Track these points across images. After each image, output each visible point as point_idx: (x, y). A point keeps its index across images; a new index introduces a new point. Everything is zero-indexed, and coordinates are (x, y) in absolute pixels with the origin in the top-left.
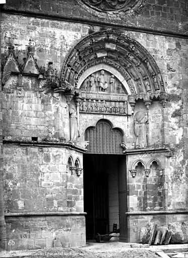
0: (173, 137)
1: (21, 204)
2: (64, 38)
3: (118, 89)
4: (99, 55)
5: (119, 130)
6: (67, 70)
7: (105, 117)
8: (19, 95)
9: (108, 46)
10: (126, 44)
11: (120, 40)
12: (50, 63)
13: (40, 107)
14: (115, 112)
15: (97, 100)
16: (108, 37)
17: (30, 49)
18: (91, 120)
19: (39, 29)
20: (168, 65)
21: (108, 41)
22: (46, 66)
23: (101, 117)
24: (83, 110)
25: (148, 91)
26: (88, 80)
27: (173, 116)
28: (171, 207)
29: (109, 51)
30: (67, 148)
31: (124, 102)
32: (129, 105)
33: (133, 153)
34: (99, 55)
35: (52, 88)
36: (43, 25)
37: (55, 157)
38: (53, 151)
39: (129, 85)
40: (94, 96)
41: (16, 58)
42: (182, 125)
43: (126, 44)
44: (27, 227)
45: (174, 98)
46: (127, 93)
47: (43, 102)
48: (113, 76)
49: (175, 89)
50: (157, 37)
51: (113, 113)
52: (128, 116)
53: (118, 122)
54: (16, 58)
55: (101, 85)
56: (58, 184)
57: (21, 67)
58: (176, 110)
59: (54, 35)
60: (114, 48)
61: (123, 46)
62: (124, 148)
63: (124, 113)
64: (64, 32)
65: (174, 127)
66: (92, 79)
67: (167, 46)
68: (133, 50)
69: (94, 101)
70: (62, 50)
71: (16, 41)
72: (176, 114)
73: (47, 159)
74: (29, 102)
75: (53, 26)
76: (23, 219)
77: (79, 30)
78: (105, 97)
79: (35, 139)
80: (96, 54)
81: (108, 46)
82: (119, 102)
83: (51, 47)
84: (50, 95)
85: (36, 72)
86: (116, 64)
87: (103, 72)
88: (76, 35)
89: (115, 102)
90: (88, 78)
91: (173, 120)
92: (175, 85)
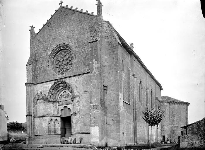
0: (77, 109)
1: (38, 132)
4: (60, 88)
7: (65, 106)
9: (61, 85)
13: (44, 107)
18: (62, 107)
20: (76, 86)
23: (64, 106)
27: (77, 102)
28: (75, 132)
34: (60, 88)
37: (45, 119)
38: (45, 118)
40: (62, 100)
44: (39, 138)
45: (77, 96)
49: (78, 93)
50: (72, 78)
53: (69, 106)
56: (46, 127)
57: (39, 97)
67: (75, 80)
71: (38, 91)
72: (78, 102)
73: (44, 120)
74: (42, 106)
75: (46, 84)
76: (39, 136)
78: (65, 100)
79: (43, 115)
91: (77, 104)
92: (77, 92)
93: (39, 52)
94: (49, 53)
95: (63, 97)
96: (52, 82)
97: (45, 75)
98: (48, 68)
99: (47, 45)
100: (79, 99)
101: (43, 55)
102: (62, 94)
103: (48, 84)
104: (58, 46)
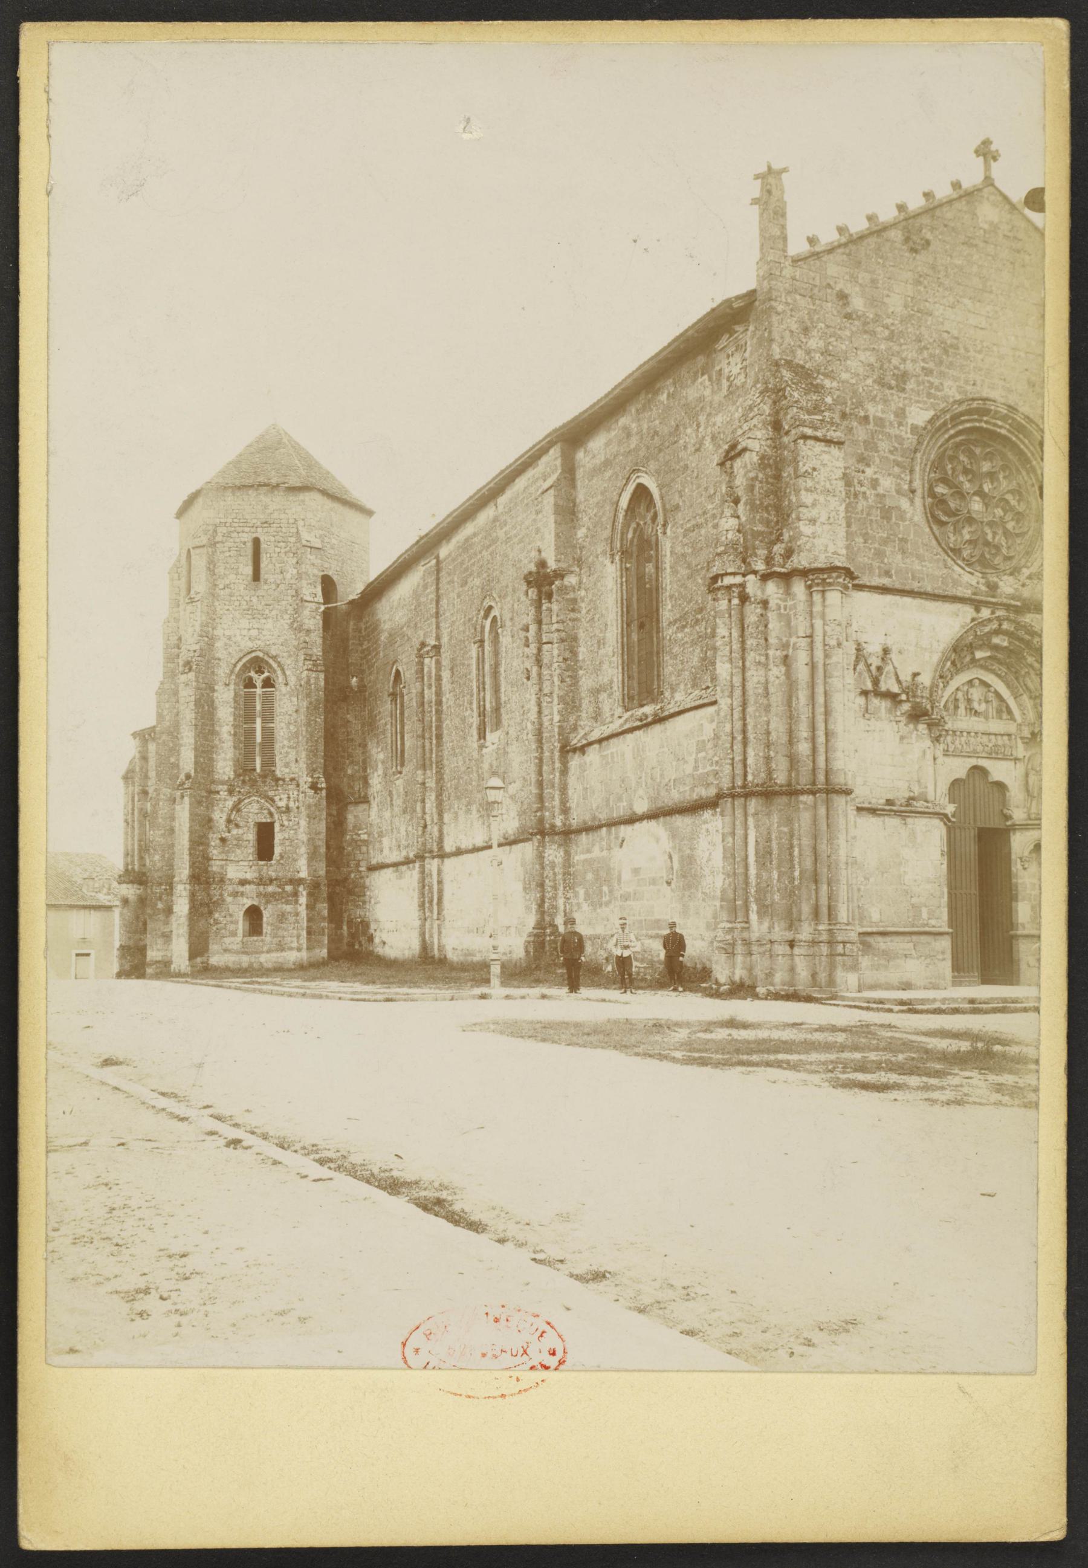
2: (934, 629)
3: (999, 712)
4: (979, 655)
5: (1001, 786)
7: (982, 763)
8: (867, 728)
10: (1027, 637)
11: (1017, 630)
12: (915, 675)
14: (995, 754)
15: (969, 733)
16: (1000, 625)
17: (886, 651)
18: (959, 768)
21: (997, 632)
22: (909, 679)
23: (973, 762)
24: (947, 751)
29: (996, 648)
31: (1009, 735)
35: (917, 715)
38: (920, 824)
39: (1020, 705)
41: (868, 666)
43: (1027, 637)
46: (1013, 719)
47: (902, 738)
48: (993, 690)
51: (994, 755)
52: (1016, 760)
53: (999, 771)
54: (868, 666)
55: (976, 705)
57: (876, 682)
59: (920, 625)
60: (1005, 644)
61: (1021, 640)
62: (1008, 818)
63: (1012, 755)
77: (958, 615)
79: (889, 802)
80: (973, 653)
81: (996, 640)
82: (1002, 735)
84: (911, 726)
85: (895, 689)
86: (1000, 669)
87: (977, 682)
89: (996, 735)
93: (845, 376)
94: (919, 416)
96: (957, 606)
97: (885, 542)
98: (904, 504)
99: (904, 360)
101: (873, 410)
104: (975, 405)
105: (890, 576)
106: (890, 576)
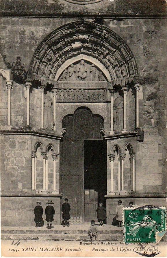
6: (36, 62)
14: (94, 99)
19: (9, 27)
25: (125, 76)
26: (66, 71)
29: (83, 41)
30: (31, 135)
32: (108, 91)
33: (111, 138)
36: (14, 23)
42: (158, 107)
51: (91, 101)
55: (80, 74)
58: (152, 93)
64: (33, 29)
65: (149, 111)
66: (71, 70)
68: (106, 37)
69: (72, 90)
70: (31, 46)
73: (13, 145)
83: (21, 43)
86: (94, 53)
87: (83, 62)
88: (46, 29)
90: (67, 68)
95: (74, 77)
100: (158, 89)
102: (70, 66)
103: (30, 25)
105: (13, 8)
106: (13, 8)
